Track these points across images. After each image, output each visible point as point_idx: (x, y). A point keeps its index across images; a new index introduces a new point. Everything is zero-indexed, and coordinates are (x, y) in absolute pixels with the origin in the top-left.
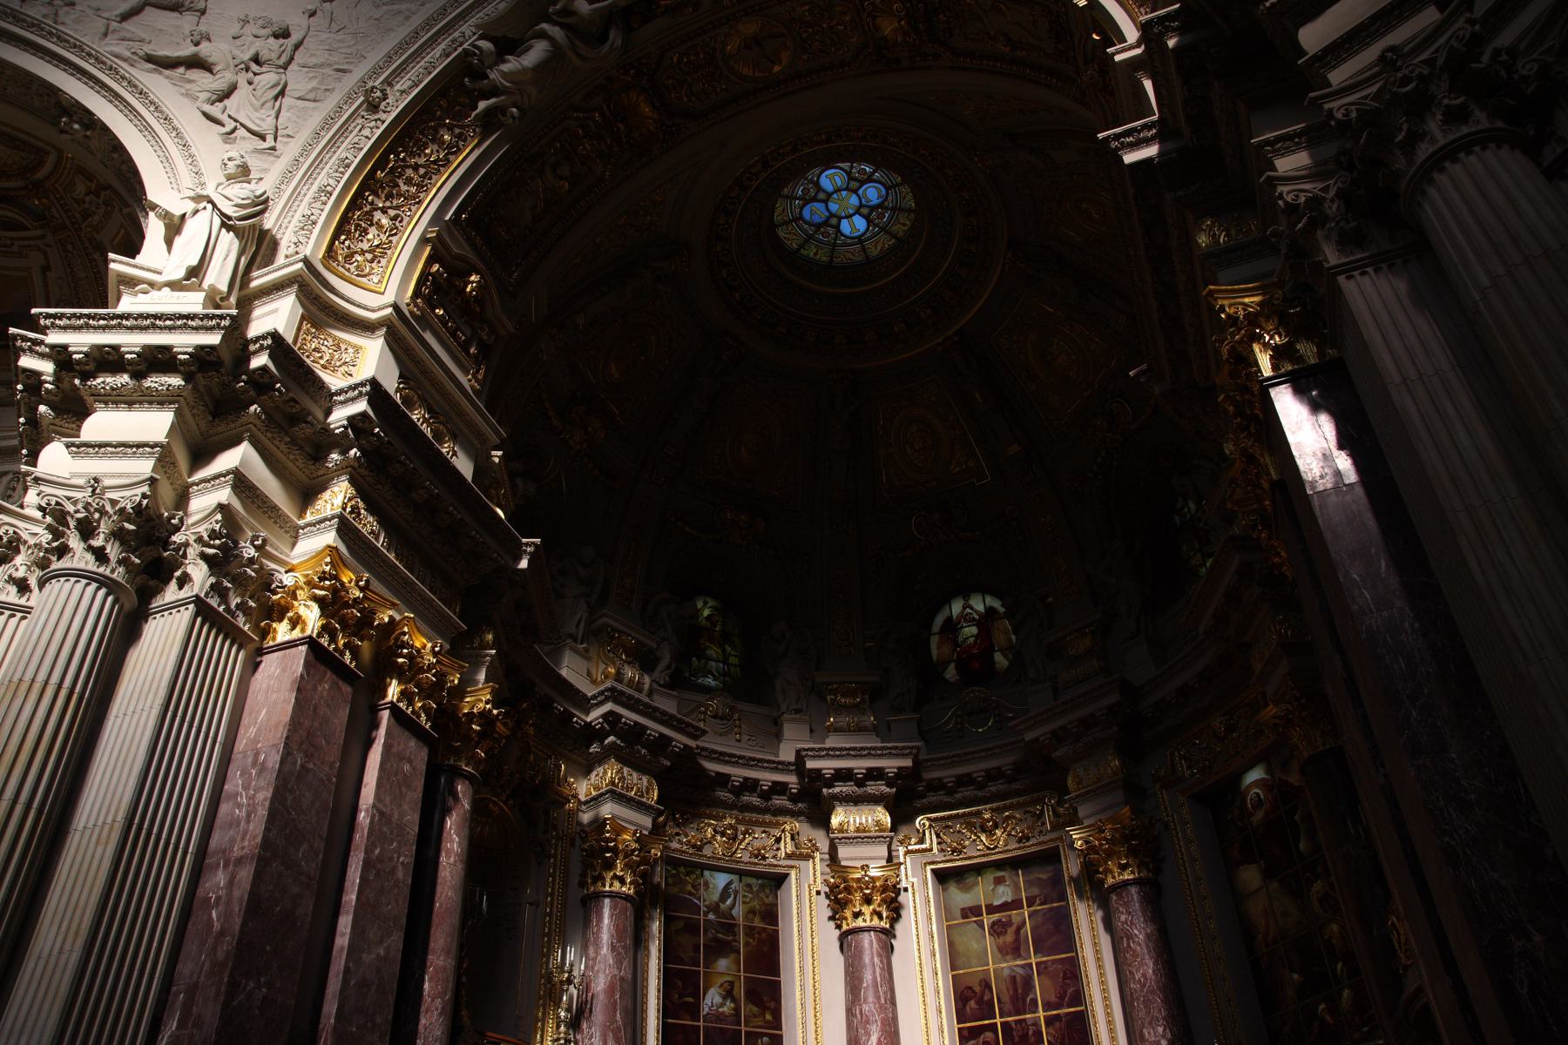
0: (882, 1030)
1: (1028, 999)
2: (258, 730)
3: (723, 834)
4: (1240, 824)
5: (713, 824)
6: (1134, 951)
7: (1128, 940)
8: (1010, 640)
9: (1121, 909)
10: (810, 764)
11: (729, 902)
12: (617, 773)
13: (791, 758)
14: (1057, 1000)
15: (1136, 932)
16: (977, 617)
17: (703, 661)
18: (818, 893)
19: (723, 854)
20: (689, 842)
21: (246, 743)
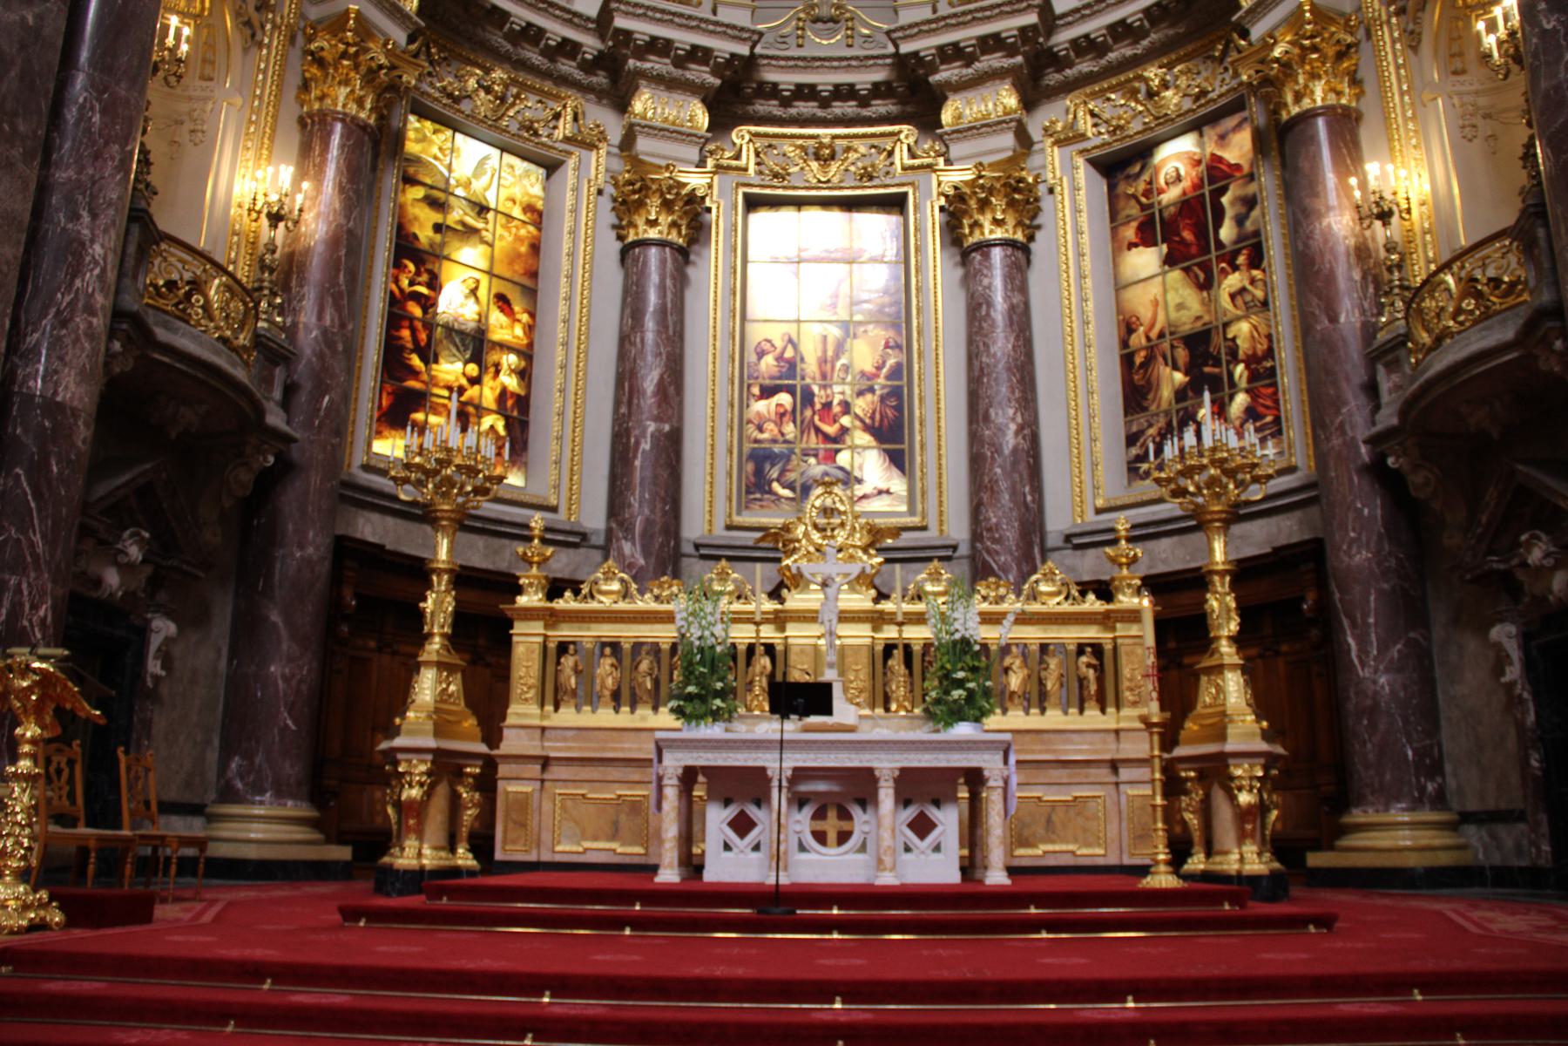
0: (667, 366)
1: (838, 365)
3: (488, 90)
4: (1144, 200)
6: (993, 321)
9: (985, 271)
10: (620, 22)
11: (485, 180)
14: (874, 370)
18: (600, 192)
20: (444, 88)
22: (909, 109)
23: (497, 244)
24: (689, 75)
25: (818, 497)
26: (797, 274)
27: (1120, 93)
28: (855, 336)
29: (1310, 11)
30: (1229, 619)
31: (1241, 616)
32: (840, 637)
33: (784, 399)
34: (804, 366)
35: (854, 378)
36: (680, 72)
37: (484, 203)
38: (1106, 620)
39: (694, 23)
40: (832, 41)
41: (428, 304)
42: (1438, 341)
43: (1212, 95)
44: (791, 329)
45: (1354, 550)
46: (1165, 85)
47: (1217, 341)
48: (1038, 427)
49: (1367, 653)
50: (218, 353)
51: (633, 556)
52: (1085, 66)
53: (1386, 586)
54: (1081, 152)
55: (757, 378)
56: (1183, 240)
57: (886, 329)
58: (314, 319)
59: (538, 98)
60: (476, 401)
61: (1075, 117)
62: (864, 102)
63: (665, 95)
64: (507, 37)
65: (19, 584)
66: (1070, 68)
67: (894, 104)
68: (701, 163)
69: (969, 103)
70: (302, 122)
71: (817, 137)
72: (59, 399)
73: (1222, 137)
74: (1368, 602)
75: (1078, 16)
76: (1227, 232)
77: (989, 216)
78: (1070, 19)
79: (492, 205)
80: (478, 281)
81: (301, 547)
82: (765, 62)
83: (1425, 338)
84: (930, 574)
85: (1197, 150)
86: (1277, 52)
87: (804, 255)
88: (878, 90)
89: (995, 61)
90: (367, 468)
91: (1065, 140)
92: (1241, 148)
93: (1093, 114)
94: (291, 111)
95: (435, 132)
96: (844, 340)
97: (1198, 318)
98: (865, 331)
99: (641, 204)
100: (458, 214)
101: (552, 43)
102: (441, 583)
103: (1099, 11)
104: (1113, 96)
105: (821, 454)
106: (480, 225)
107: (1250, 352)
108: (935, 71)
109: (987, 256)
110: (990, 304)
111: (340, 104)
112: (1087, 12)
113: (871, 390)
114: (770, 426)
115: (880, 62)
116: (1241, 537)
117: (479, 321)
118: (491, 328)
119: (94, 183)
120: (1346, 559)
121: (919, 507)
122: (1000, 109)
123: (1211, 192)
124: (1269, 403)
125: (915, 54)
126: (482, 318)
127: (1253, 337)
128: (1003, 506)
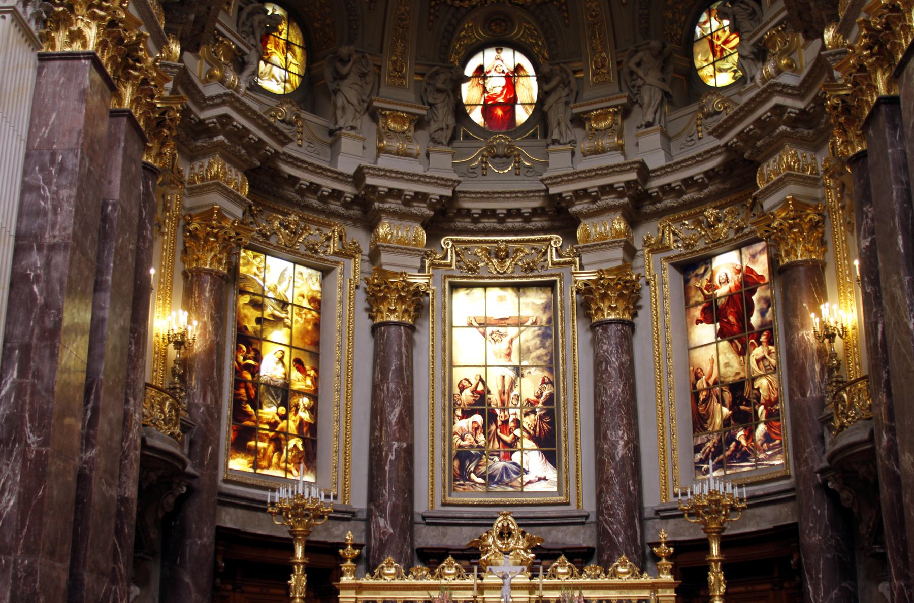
0: (403, 405)
1: (512, 395)
2: (51, 131)
3: (286, 228)
4: (706, 292)
5: (279, 218)
6: (610, 373)
7: (607, 364)
8: (532, 98)
9: (604, 341)
10: (369, 181)
12: (222, 167)
13: (351, 170)
14: (535, 399)
15: (614, 359)
16: (506, 71)
17: (269, 65)
18: (357, 287)
19: (285, 245)
20: (260, 231)
21: (39, 142)
22: (556, 224)
23: (294, 326)
24: (413, 210)
25: (500, 522)
26: (484, 334)
27: (691, 220)
28: (523, 376)
29: (792, 204)
30: (720, 585)
31: (726, 584)
32: (512, 598)
33: (478, 418)
34: (489, 396)
35: (522, 404)
36: (408, 208)
37: (285, 300)
38: (654, 587)
39: (416, 178)
40: (506, 171)
41: (255, 370)
42: (842, 426)
43: (746, 231)
44: (481, 371)
45: (812, 534)
46: (718, 220)
47: (747, 388)
48: (638, 441)
49: (818, 595)
50: (171, 443)
51: (386, 527)
52: (669, 202)
53: (829, 556)
54: (667, 259)
55: (460, 404)
56: (729, 320)
57: (543, 371)
58: (201, 401)
59: (316, 227)
60: (285, 430)
61: (663, 234)
62: (527, 220)
63: (399, 222)
64: (297, 192)
65: (116, 590)
66: (660, 202)
67: (546, 221)
68: (422, 269)
69: (595, 227)
70: (185, 274)
71: (496, 242)
72: (126, 496)
73: (753, 256)
74: (819, 564)
75: (663, 171)
76: (755, 320)
77: (607, 304)
78: (659, 173)
79: (290, 301)
80: (283, 352)
81: (200, 538)
82: (462, 195)
83: (837, 423)
84: (560, 563)
85: (739, 263)
86: (775, 224)
87: (488, 322)
88: (535, 212)
89: (610, 200)
90: (226, 481)
91: (657, 249)
92: (764, 265)
93: (674, 234)
94: (179, 267)
95: (255, 257)
96: (516, 379)
97: (738, 373)
98: (530, 372)
99: (385, 298)
100: (271, 309)
101: (325, 193)
102: (299, 570)
103: (677, 170)
104: (687, 223)
105: (502, 454)
106: (283, 315)
107: (767, 399)
108: (573, 205)
109: (605, 330)
110: (608, 363)
111: (208, 263)
112: (669, 169)
113: (534, 412)
114: (470, 436)
115: (537, 194)
116: (760, 516)
117: (285, 378)
118: (293, 382)
119: (134, 382)
120: (808, 539)
121: (564, 490)
122: (614, 232)
123: (745, 291)
124: (777, 432)
125: (560, 195)
126: (287, 376)
127: (769, 389)
128: (615, 493)
